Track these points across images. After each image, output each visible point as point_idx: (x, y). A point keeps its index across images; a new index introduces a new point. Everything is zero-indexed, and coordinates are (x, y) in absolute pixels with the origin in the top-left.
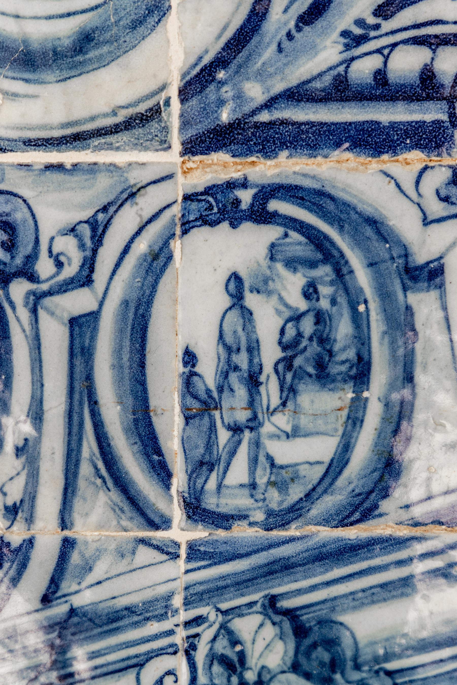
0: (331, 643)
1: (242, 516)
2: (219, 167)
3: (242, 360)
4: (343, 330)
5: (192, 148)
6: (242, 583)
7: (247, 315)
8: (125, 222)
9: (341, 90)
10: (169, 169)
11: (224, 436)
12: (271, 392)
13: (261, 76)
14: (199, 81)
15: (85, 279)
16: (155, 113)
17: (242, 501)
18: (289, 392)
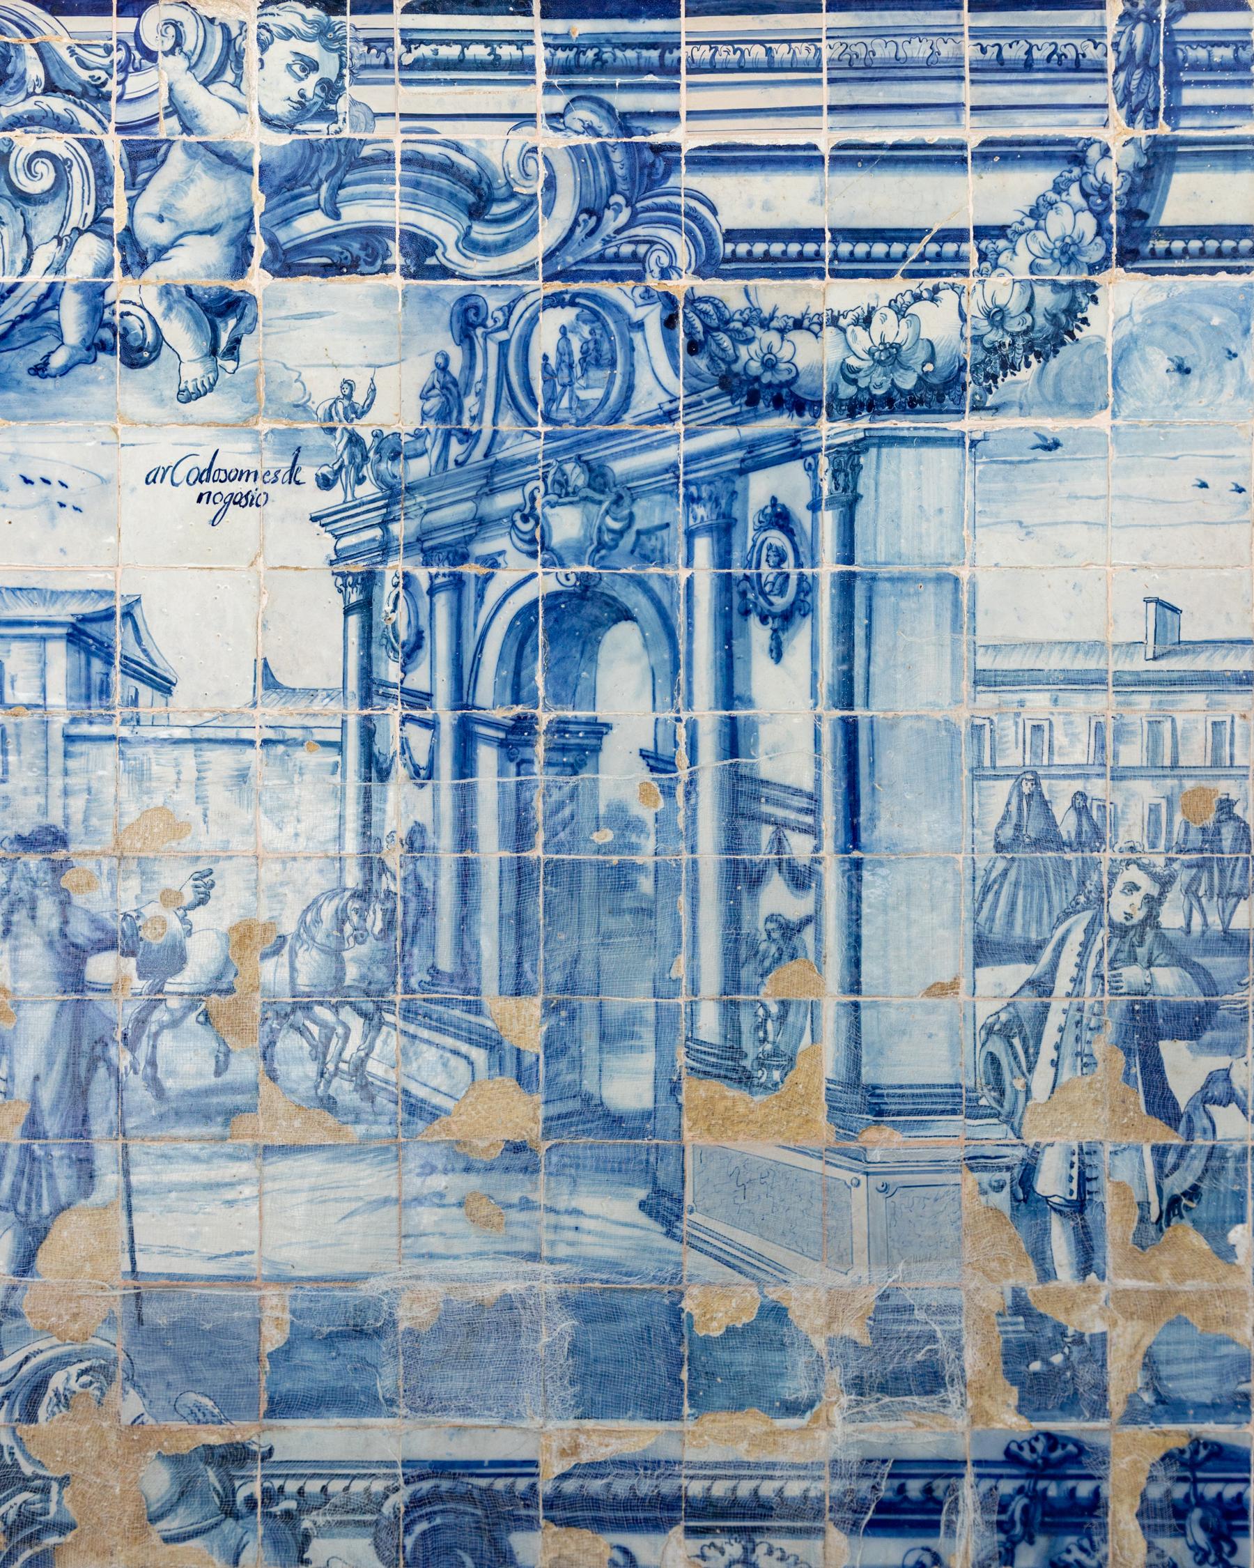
0: (603, 475)
1: (566, 421)
2: (557, 286)
3: (566, 358)
4: (606, 347)
5: (546, 279)
6: (567, 449)
7: (568, 341)
8: (521, 306)
9: (601, 259)
10: (538, 288)
11: (559, 388)
12: (578, 371)
13: (572, 254)
14: (549, 256)
15: (505, 327)
16: (533, 267)
17: (566, 415)
18: (585, 371)
